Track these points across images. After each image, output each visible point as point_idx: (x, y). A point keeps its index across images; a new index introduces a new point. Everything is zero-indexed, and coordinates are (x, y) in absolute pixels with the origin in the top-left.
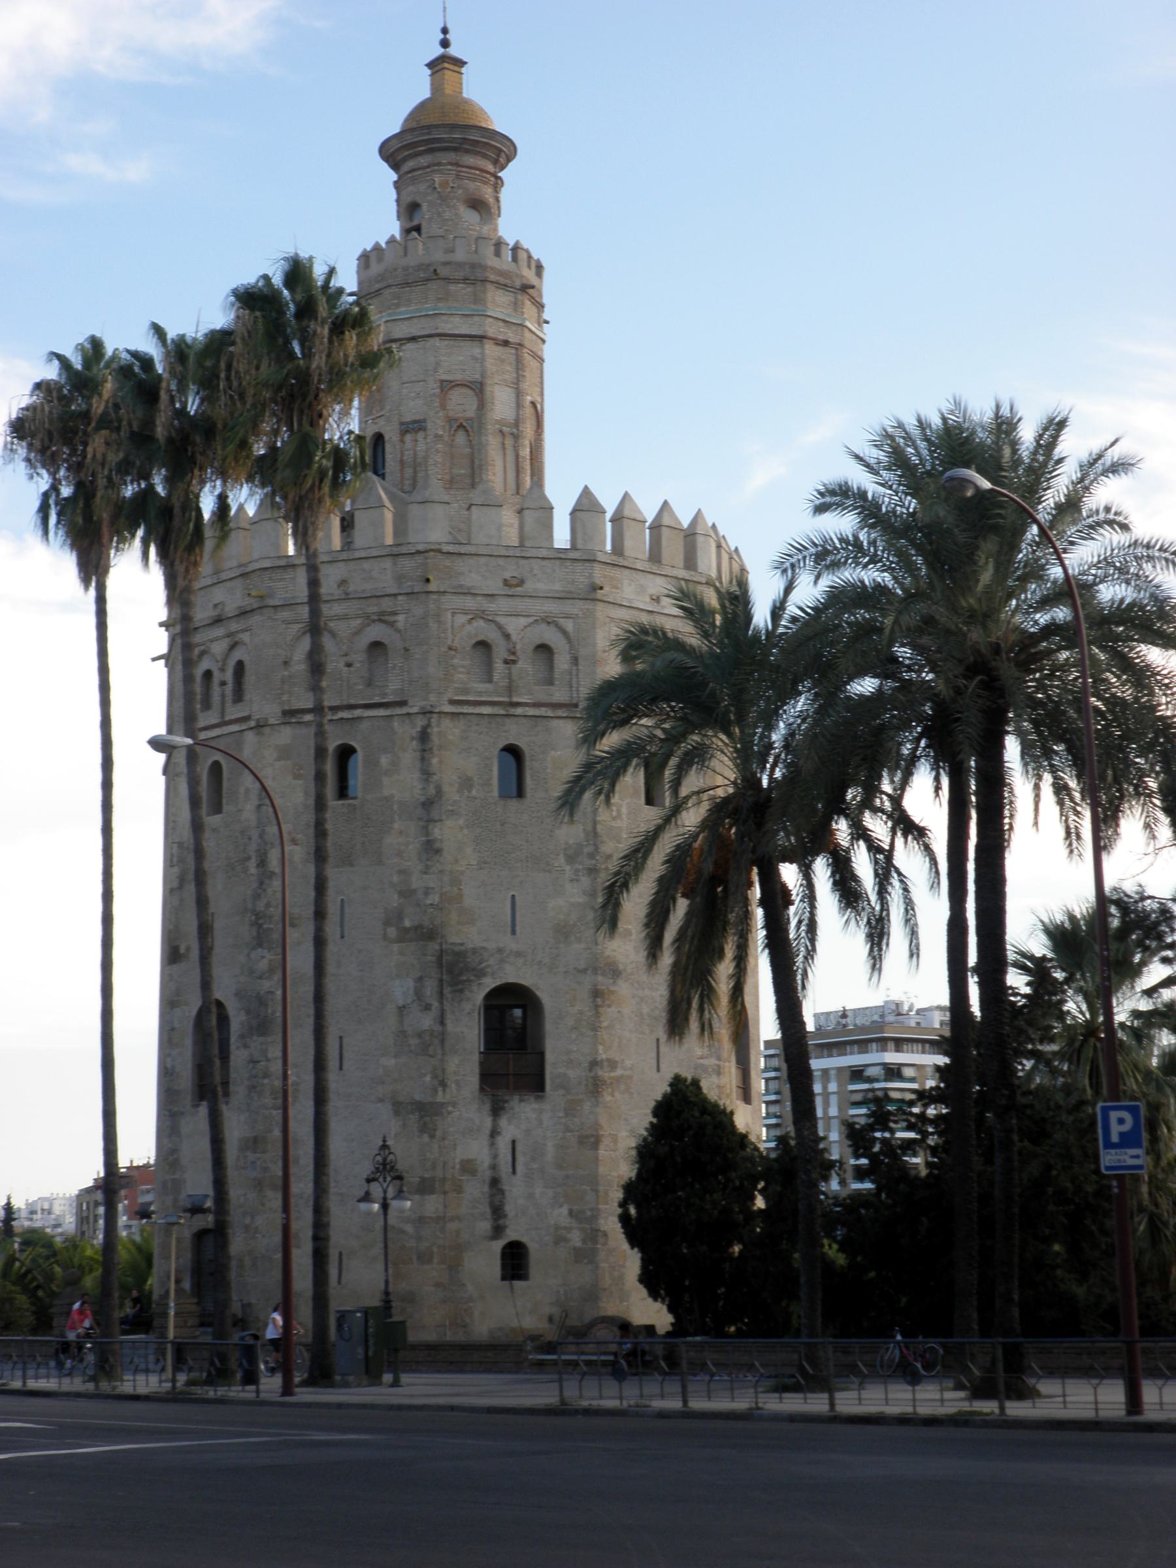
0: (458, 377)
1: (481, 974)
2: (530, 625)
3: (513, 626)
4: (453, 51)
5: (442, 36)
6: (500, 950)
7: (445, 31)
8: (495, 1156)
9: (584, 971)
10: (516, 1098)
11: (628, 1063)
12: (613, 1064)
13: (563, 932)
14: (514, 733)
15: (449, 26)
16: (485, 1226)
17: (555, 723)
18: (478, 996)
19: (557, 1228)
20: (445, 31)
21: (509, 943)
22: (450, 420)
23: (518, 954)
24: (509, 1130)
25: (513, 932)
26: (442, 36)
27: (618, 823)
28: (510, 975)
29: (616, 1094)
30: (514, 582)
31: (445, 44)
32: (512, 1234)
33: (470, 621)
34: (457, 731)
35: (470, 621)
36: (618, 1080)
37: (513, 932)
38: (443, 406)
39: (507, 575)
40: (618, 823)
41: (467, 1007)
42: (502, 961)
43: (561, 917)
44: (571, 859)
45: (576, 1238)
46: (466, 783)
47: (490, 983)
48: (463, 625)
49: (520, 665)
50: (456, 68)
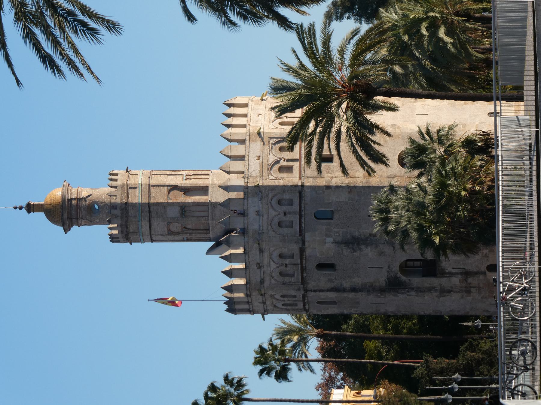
0: (166, 229)
1: (396, 277)
2: (274, 262)
4: (24, 205)
5: (18, 209)
6: (388, 272)
7: (15, 208)
13: (381, 254)
15: (13, 206)
16: (481, 277)
17: (307, 254)
18: (403, 278)
19: (482, 256)
20: (15, 208)
21: (385, 270)
23: (389, 267)
24: (449, 269)
25: (382, 268)
26: (18, 209)
27: (341, 233)
28: (396, 268)
30: (258, 266)
31: (21, 208)
32: (483, 268)
33: (273, 277)
34: (312, 283)
35: (273, 277)
37: (382, 268)
39: (256, 268)
40: (341, 233)
42: (391, 271)
43: (376, 254)
44: (355, 251)
46: (330, 280)
47: (399, 275)
48: (275, 280)
49: (287, 263)
50: (32, 207)
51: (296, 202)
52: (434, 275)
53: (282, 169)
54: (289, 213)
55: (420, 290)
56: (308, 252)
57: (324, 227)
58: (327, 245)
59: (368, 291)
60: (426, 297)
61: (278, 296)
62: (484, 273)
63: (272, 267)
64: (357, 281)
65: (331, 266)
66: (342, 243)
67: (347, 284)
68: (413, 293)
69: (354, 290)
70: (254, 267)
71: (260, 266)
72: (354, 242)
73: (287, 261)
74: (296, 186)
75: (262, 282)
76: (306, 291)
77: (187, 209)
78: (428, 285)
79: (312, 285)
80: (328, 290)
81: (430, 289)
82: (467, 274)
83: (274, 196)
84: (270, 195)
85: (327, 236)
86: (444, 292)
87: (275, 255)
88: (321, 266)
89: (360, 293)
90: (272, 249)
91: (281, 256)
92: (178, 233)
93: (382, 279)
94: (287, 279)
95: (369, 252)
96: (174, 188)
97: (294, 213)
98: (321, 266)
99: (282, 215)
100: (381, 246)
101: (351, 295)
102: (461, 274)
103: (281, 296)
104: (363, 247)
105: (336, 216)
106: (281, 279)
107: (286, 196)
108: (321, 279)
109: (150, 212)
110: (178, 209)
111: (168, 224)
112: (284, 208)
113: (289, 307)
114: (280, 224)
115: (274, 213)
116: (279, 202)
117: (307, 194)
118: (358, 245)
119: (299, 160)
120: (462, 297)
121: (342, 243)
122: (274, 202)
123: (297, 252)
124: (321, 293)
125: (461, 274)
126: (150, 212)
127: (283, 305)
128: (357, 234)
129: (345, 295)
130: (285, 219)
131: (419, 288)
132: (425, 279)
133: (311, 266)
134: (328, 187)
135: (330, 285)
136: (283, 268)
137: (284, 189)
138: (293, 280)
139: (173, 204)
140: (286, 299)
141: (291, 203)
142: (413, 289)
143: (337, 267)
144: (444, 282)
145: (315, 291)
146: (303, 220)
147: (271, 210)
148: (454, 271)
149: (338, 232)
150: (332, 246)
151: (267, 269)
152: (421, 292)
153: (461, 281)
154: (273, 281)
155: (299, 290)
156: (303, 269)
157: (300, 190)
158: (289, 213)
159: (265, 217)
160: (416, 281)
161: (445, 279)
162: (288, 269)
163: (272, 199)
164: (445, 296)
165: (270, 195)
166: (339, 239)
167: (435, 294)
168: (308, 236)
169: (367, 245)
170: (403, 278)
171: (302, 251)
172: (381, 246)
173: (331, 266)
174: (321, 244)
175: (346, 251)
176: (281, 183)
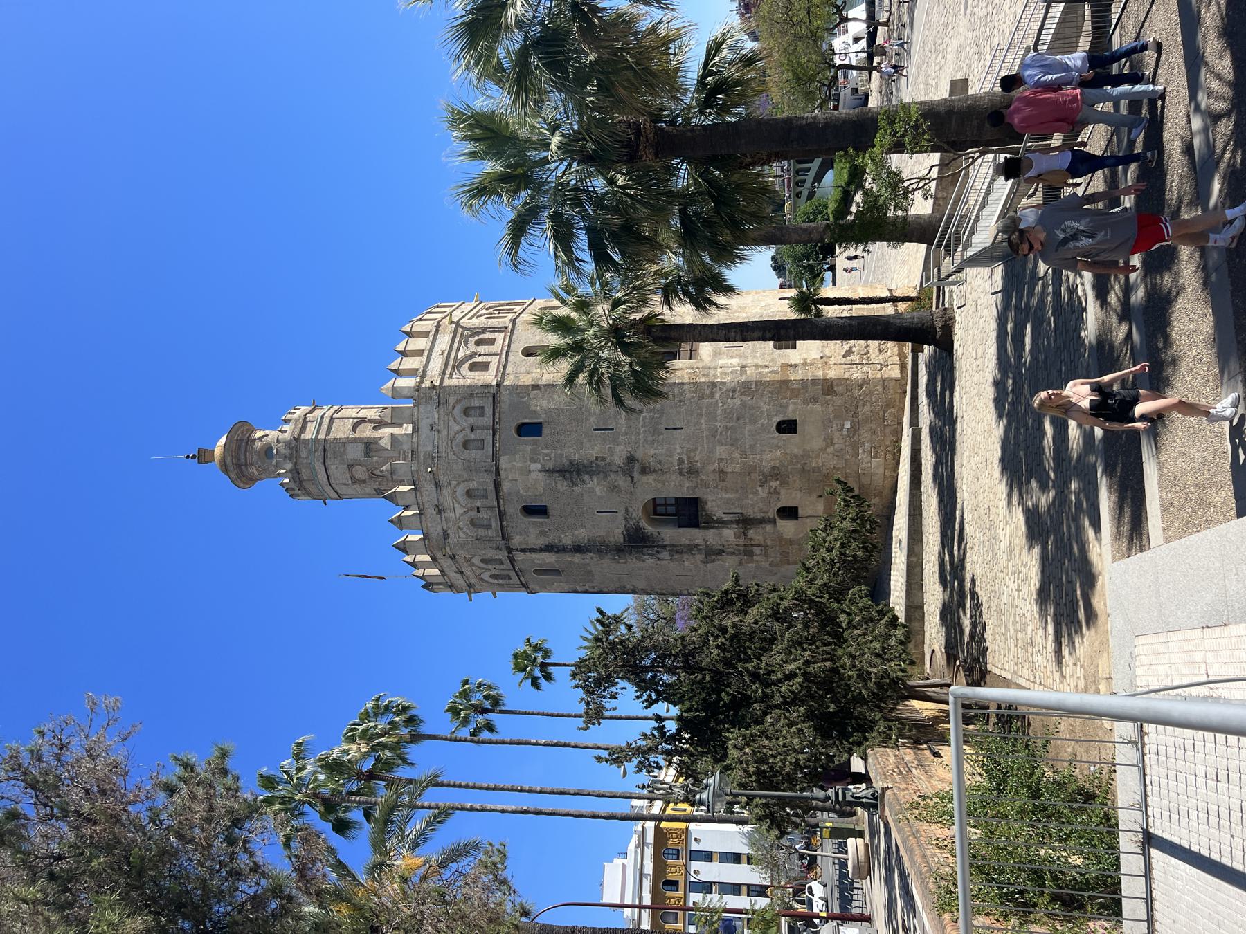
1: (638, 529)
3: (459, 510)
8: (731, 522)
9: (632, 478)
10: (700, 511)
11: (679, 451)
12: (681, 461)
13: (614, 488)
14: (513, 510)
16: (769, 528)
21: (621, 515)
22: (371, 478)
23: (627, 511)
24: (718, 514)
28: (637, 512)
29: (697, 458)
32: (772, 513)
36: (689, 458)
38: (364, 482)
41: (655, 534)
44: (575, 484)
45: (775, 484)
51: (489, 411)
52: (695, 525)
53: (473, 367)
54: (478, 428)
55: (676, 550)
56: (506, 486)
57: (529, 448)
58: (534, 476)
59: (599, 551)
60: (686, 563)
61: (476, 561)
62: (774, 522)
63: (458, 510)
64: (581, 535)
65: (541, 511)
66: (554, 471)
67: (567, 540)
68: (665, 555)
69: (578, 549)
70: (431, 511)
71: (440, 511)
72: (571, 471)
73: (479, 503)
74: (489, 386)
75: (446, 536)
76: (510, 550)
77: (373, 446)
78: (687, 542)
79: (517, 541)
80: (542, 550)
81: (691, 549)
82: (745, 522)
83: (458, 401)
84: (452, 400)
85: (533, 460)
86: (713, 553)
87: (461, 491)
88: (530, 511)
89: (589, 555)
90: (454, 482)
91: (469, 494)
92: (364, 482)
93: (617, 534)
94: (481, 532)
95: (595, 486)
96: (363, 421)
97: (484, 428)
98: (530, 511)
99: (468, 430)
100: (613, 476)
101: (577, 558)
102: (737, 522)
103: (483, 561)
104: (586, 477)
105: (546, 431)
106: (472, 532)
107: (475, 403)
108: (528, 532)
109: (325, 450)
110: (361, 447)
111: (350, 467)
112: (472, 420)
113: (500, 581)
114: (466, 445)
115: (457, 428)
116: (466, 411)
117: (505, 397)
118: (579, 473)
119: (499, 354)
120: (741, 564)
121: (554, 471)
122: (457, 411)
123: (491, 487)
124: (534, 555)
125: (737, 522)
126: (325, 450)
127: (491, 576)
128: (577, 458)
129: (568, 557)
130: (472, 436)
131: (673, 545)
132: (681, 530)
133: (513, 510)
134: (535, 387)
135: (542, 541)
136: (473, 514)
137: (471, 392)
138: (490, 533)
139: (355, 441)
140: (490, 567)
141: (482, 415)
142: (664, 546)
143: (551, 511)
144: (710, 537)
145: (523, 551)
146: (497, 437)
147: (452, 423)
148: (726, 517)
149: (547, 455)
150: (540, 476)
151: (450, 515)
152: (677, 552)
153: (737, 536)
154: (461, 535)
155: (499, 548)
156: (502, 515)
157: (494, 393)
158: (478, 428)
159: (444, 433)
160: (670, 534)
161: (712, 531)
162: (481, 515)
163: (454, 407)
164: (714, 561)
165: (452, 400)
166: (550, 465)
167: (700, 557)
168: (504, 462)
169: (591, 474)
170: (649, 529)
171: (497, 484)
172: (613, 476)
173: (541, 511)
174: (525, 473)
175: (562, 485)
176: (469, 382)
